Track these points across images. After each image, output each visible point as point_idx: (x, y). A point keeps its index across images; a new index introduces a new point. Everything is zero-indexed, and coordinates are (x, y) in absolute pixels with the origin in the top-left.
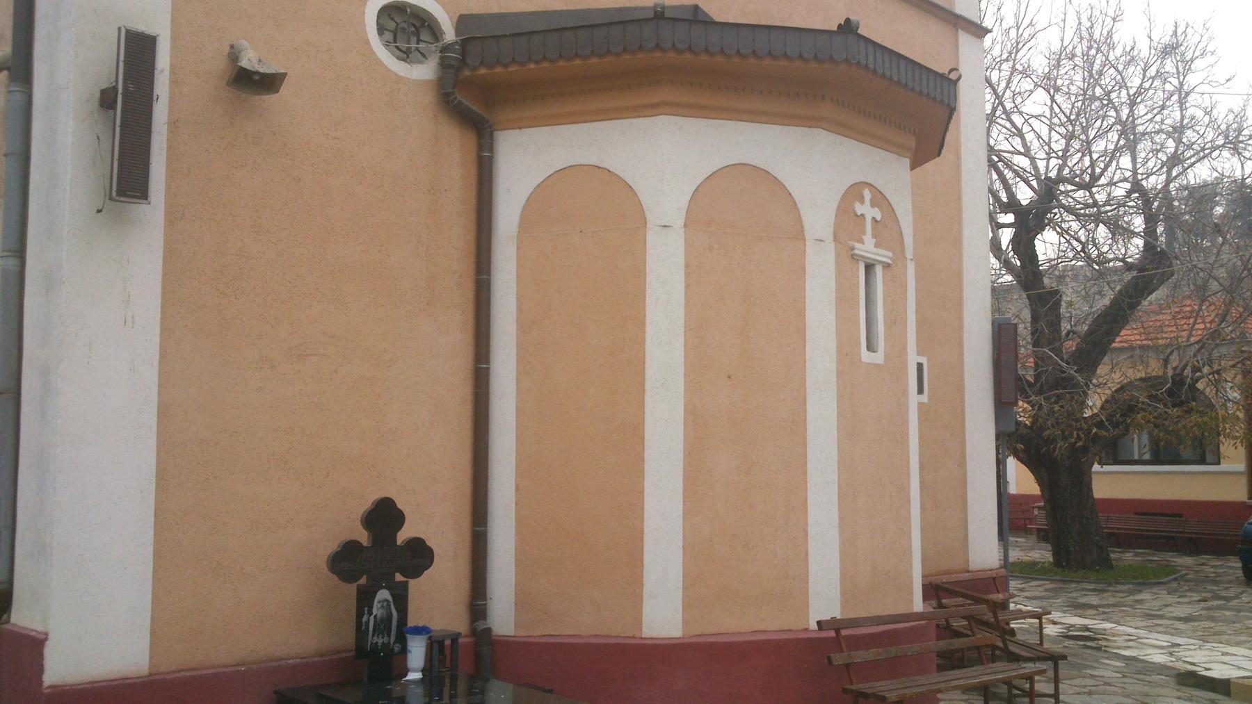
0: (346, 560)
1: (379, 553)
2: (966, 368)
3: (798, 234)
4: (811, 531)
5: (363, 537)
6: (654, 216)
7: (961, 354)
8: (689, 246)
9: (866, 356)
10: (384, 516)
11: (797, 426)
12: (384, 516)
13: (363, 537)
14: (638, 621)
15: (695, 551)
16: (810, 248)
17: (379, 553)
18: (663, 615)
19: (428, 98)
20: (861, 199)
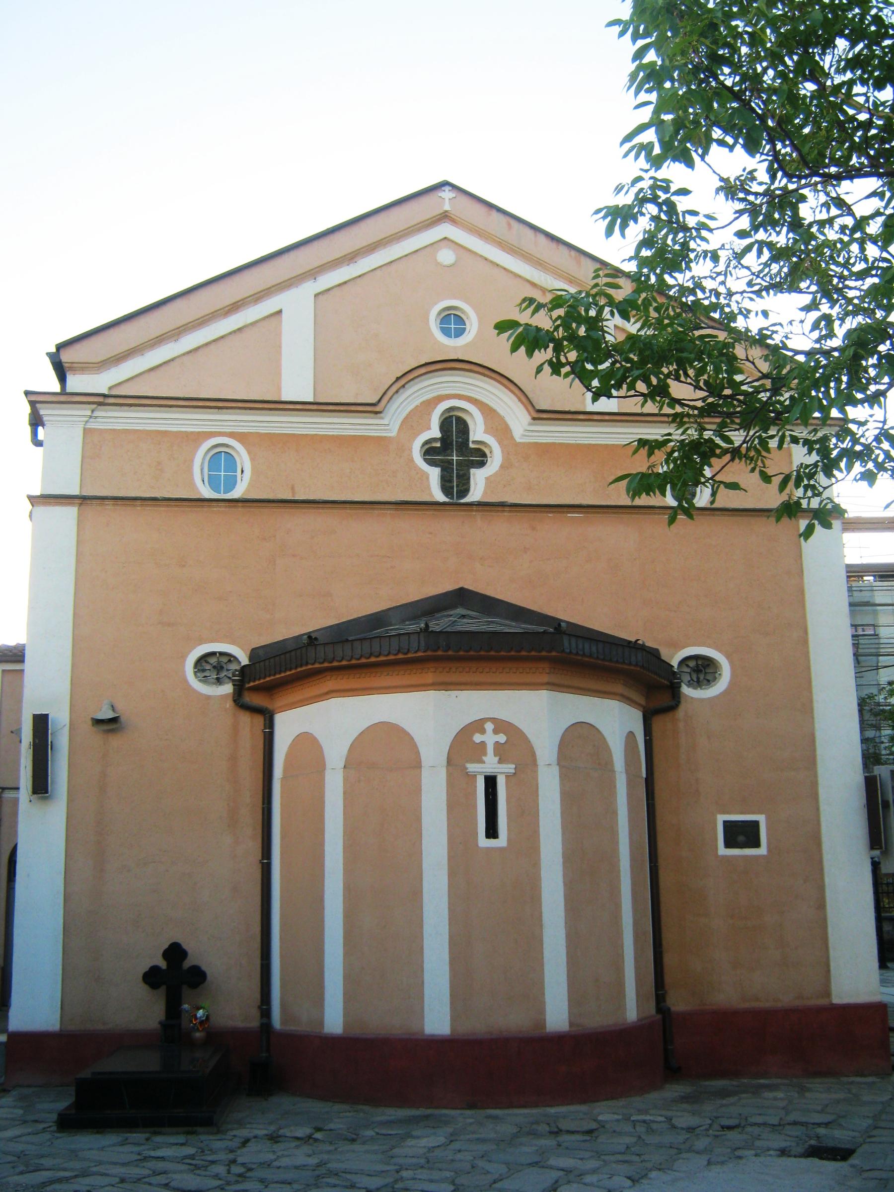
0: (152, 977)
1: (175, 975)
2: (823, 819)
3: (417, 765)
4: (427, 966)
5: (163, 964)
6: (329, 764)
7: (818, 809)
8: (346, 779)
9: (484, 842)
10: (175, 953)
11: (417, 894)
12: (175, 953)
13: (163, 964)
14: (321, 1023)
15: (349, 978)
16: (425, 774)
17: (175, 975)
18: (334, 1020)
19: (229, 704)
20: (483, 731)
